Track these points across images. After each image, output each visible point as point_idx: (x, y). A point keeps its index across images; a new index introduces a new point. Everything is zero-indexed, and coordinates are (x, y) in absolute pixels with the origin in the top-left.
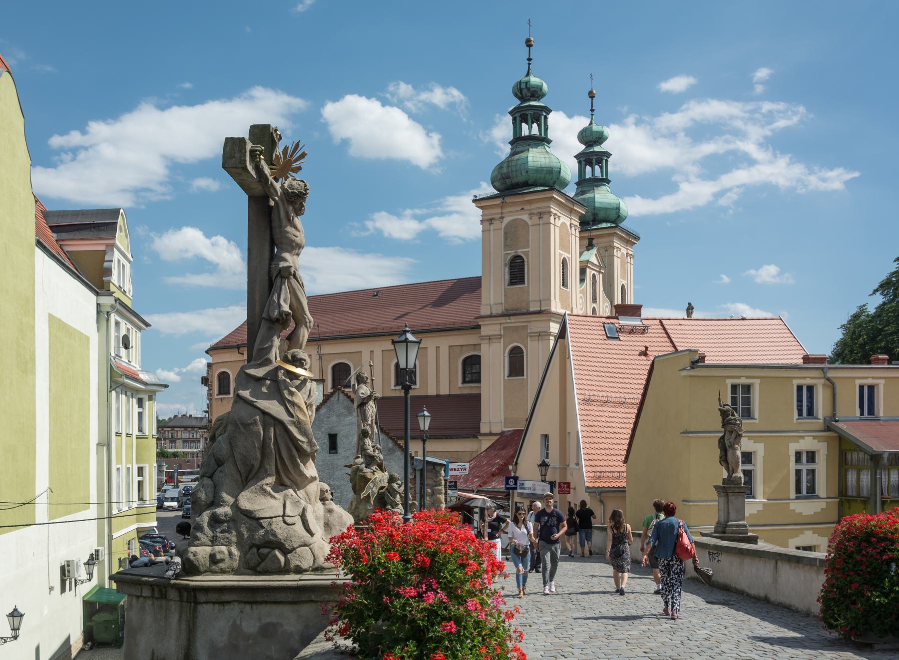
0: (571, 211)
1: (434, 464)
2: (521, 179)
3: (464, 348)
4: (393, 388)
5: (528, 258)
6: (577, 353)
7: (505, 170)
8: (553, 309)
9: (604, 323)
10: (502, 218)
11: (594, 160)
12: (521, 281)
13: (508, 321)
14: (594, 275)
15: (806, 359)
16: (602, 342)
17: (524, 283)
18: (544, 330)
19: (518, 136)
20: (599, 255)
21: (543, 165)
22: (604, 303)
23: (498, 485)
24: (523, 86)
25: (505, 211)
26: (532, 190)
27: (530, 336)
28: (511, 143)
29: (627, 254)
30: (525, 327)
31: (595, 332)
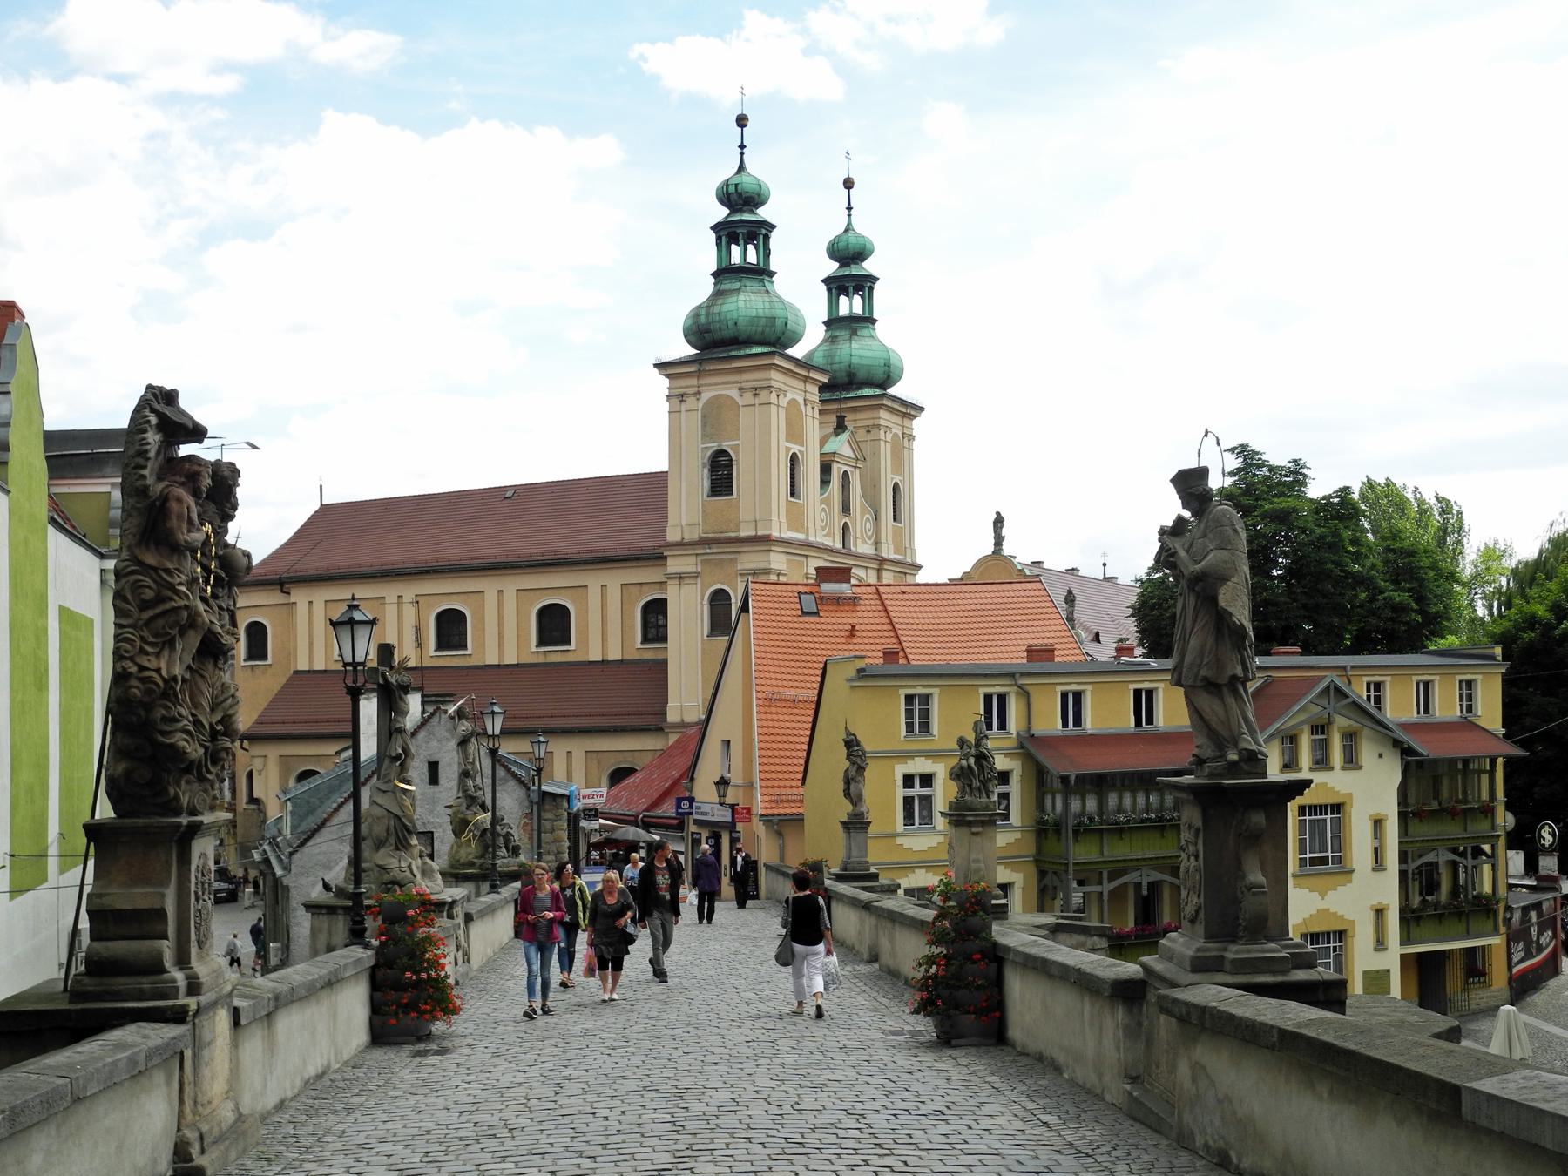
0: (806, 379)
1: (555, 796)
2: (727, 334)
3: (644, 587)
4: (534, 649)
5: (737, 456)
6: (760, 636)
7: (703, 320)
8: (775, 534)
9: (800, 593)
10: (699, 393)
11: (851, 289)
12: (730, 492)
13: (709, 551)
14: (845, 473)
15: (1032, 653)
16: (795, 619)
17: (732, 494)
18: (763, 565)
19: (724, 265)
20: (854, 443)
21: (761, 313)
22: (862, 514)
23: (668, 810)
24: (732, 189)
25: (701, 382)
26: (742, 353)
27: (741, 575)
28: (714, 275)
29: (903, 433)
30: (734, 561)
31: (787, 606)
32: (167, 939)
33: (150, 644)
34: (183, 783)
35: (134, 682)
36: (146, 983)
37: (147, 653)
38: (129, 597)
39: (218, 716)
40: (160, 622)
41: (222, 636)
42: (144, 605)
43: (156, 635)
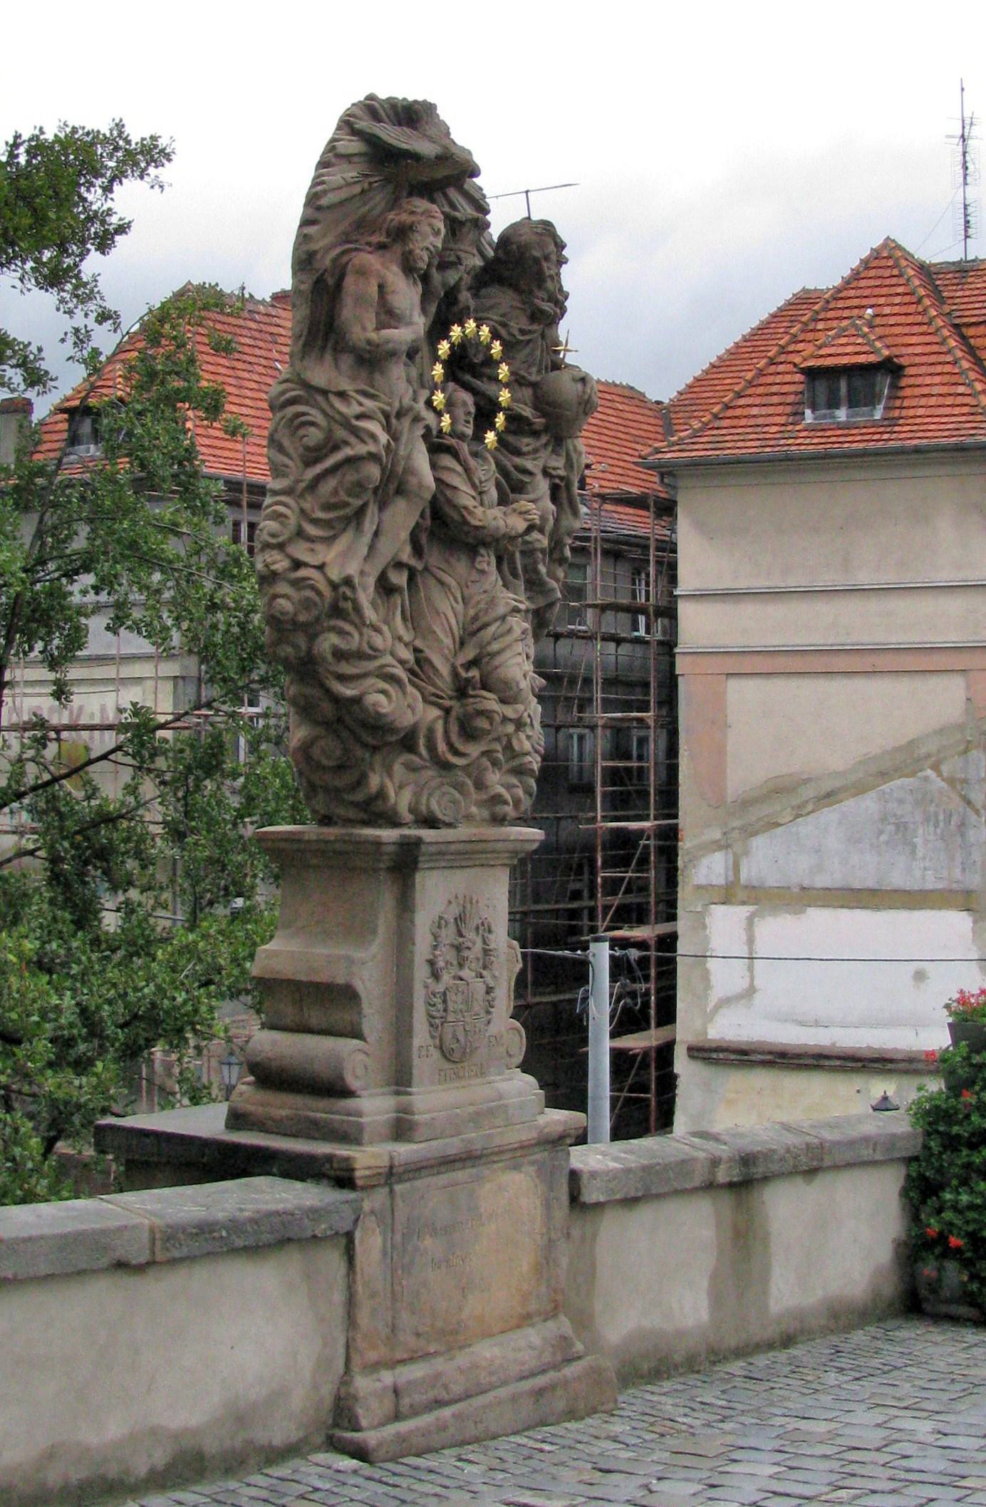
32: (357, 1034)
33: (315, 522)
34: (398, 768)
35: (282, 588)
36: (317, 1109)
37: (311, 539)
38: (286, 443)
39: (470, 653)
40: (329, 485)
41: (470, 513)
42: (312, 456)
43: (328, 507)
